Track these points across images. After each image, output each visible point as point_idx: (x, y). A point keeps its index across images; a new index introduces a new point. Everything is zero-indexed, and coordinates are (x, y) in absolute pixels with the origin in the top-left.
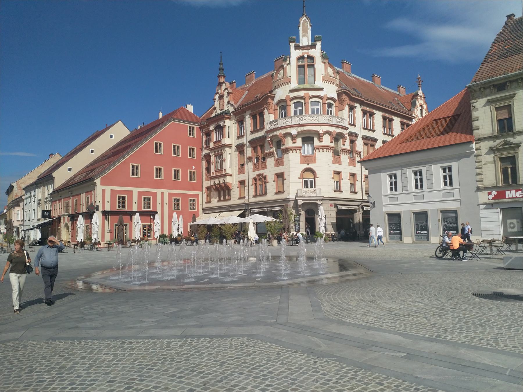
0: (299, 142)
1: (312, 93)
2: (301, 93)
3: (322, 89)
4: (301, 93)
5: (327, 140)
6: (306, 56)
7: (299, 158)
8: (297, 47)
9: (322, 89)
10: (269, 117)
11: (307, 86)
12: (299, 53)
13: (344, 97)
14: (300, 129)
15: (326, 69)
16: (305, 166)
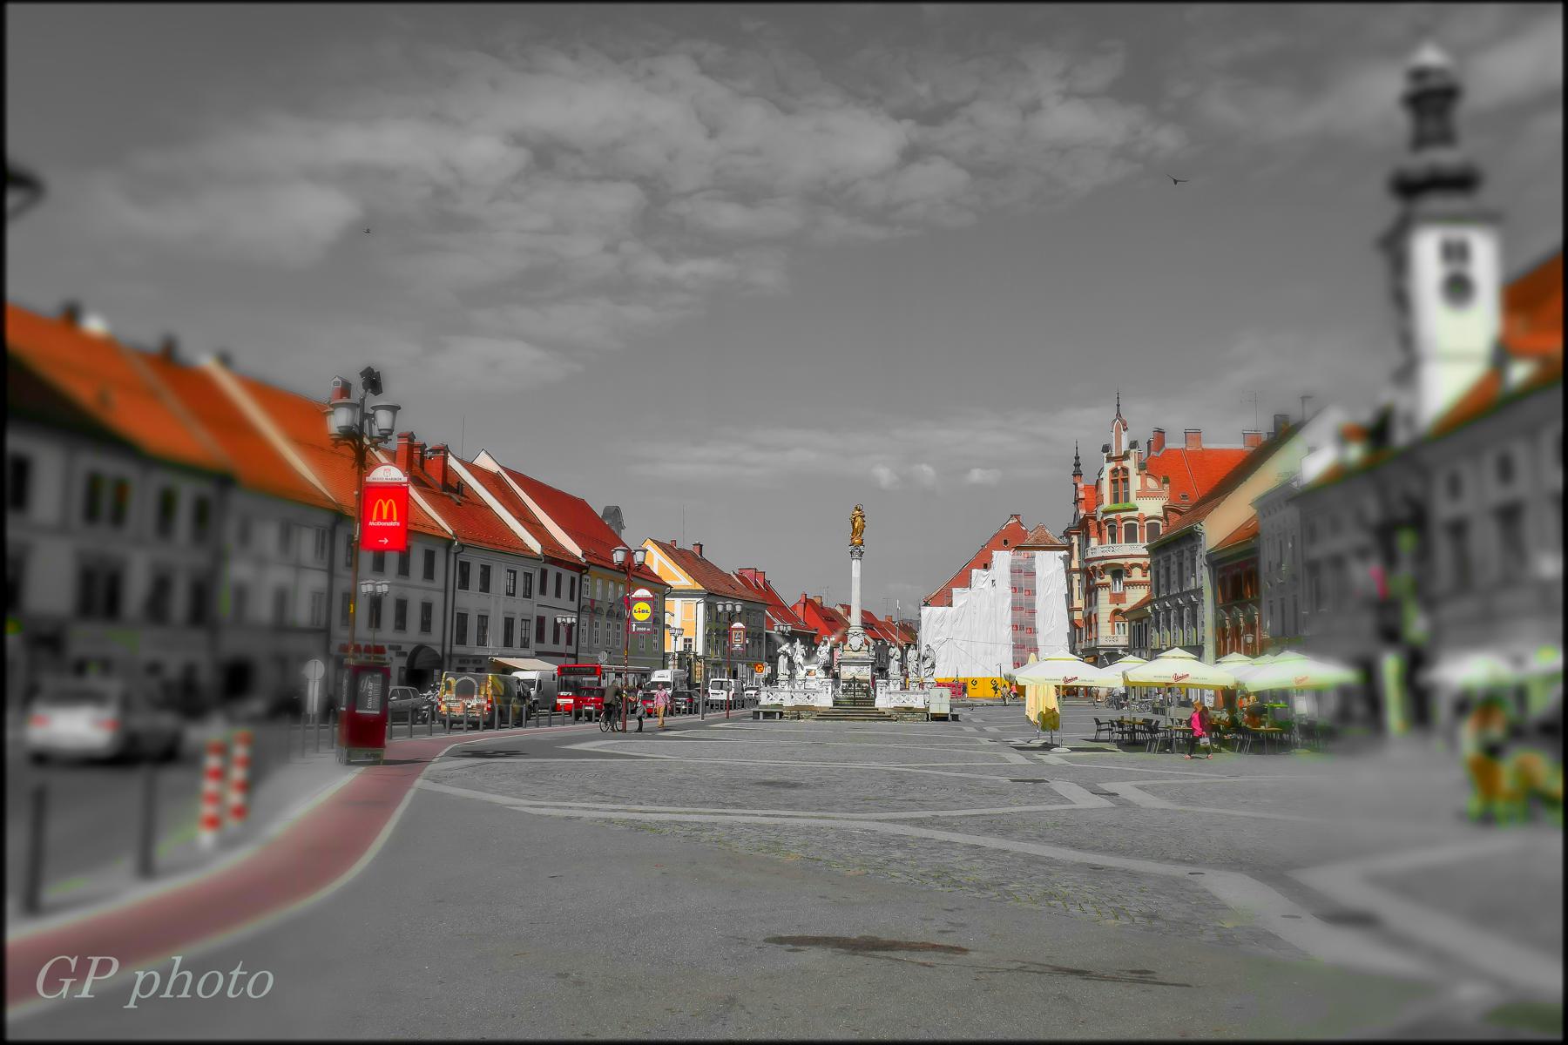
0: (1108, 578)
1: (1123, 515)
2: (1113, 516)
3: (1136, 509)
4: (1113, 516)
5: (1137, 575)
6: (1119, 468)
7: (1108, 597)
8: (1110, 459)
9: (1136, 509)
10: (1094, 542)
11: (1118, 506)
12: (1113, 465)
13: (1170, 514)
14: (1103, 562)
15: (1143, 482)
16: (1114, 606)
